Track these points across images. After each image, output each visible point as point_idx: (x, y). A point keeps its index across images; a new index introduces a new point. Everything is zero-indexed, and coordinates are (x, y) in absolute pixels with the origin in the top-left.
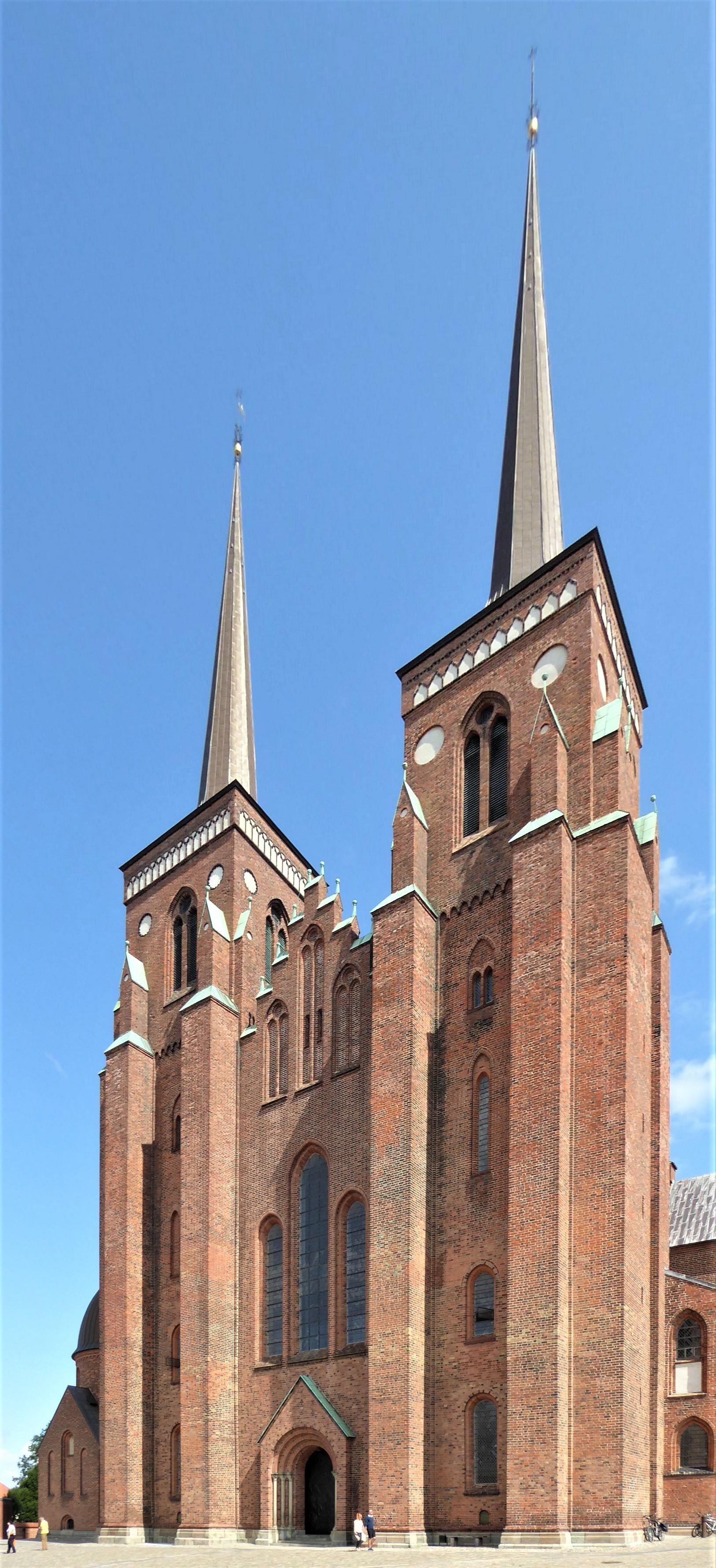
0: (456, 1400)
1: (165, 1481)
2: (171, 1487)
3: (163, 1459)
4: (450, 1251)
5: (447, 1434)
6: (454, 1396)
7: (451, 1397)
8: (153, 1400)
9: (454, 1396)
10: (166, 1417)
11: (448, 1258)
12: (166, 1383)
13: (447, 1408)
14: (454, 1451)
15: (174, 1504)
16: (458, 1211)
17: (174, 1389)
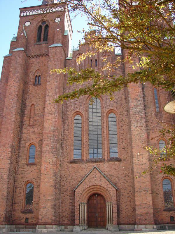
0: (157, 178)
1: (20, 204)
2: (22, 207)
3: (19, 195)
4: (151, 132)
5: (155, 190)
6: (157, 177)
7: (156, 177)
8: (15, 171)
9: (157, 177)
10: (22, 178)
11: (150, 134)
12: (23, 164)
13: (154, 181)
14: (158, 195)
15: (24, 215)
16: (152, 121)
17: (27, 167)
